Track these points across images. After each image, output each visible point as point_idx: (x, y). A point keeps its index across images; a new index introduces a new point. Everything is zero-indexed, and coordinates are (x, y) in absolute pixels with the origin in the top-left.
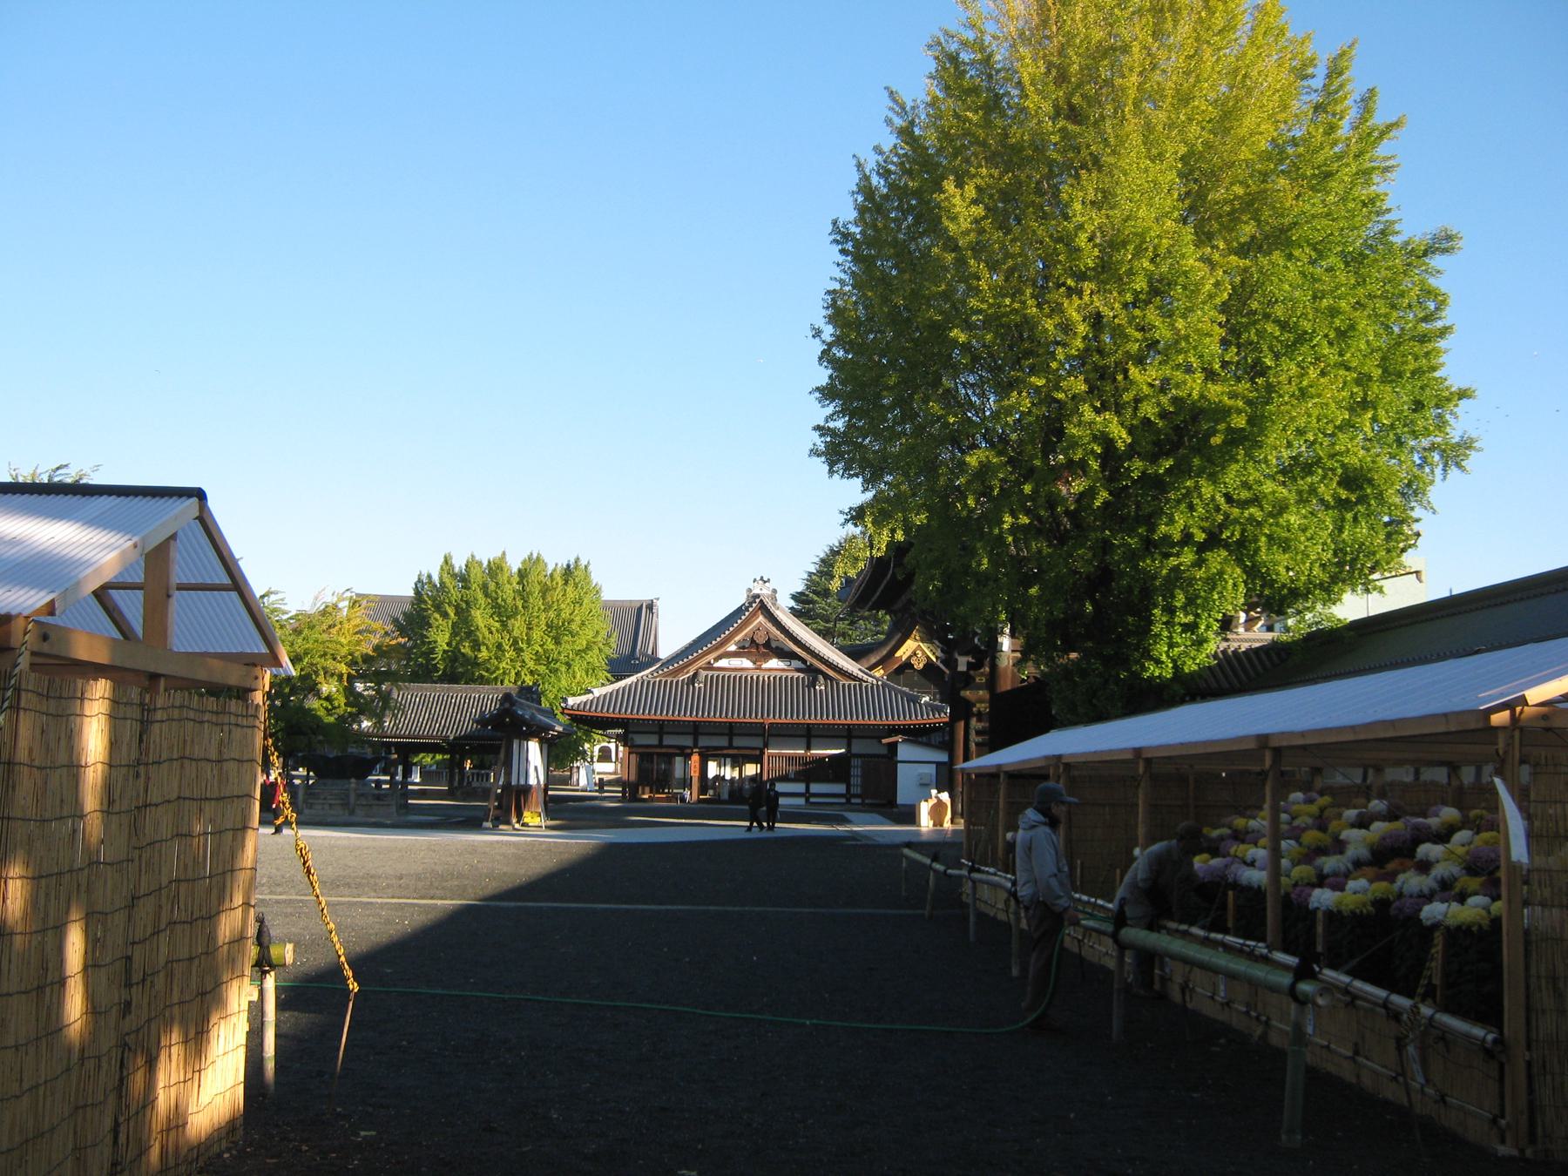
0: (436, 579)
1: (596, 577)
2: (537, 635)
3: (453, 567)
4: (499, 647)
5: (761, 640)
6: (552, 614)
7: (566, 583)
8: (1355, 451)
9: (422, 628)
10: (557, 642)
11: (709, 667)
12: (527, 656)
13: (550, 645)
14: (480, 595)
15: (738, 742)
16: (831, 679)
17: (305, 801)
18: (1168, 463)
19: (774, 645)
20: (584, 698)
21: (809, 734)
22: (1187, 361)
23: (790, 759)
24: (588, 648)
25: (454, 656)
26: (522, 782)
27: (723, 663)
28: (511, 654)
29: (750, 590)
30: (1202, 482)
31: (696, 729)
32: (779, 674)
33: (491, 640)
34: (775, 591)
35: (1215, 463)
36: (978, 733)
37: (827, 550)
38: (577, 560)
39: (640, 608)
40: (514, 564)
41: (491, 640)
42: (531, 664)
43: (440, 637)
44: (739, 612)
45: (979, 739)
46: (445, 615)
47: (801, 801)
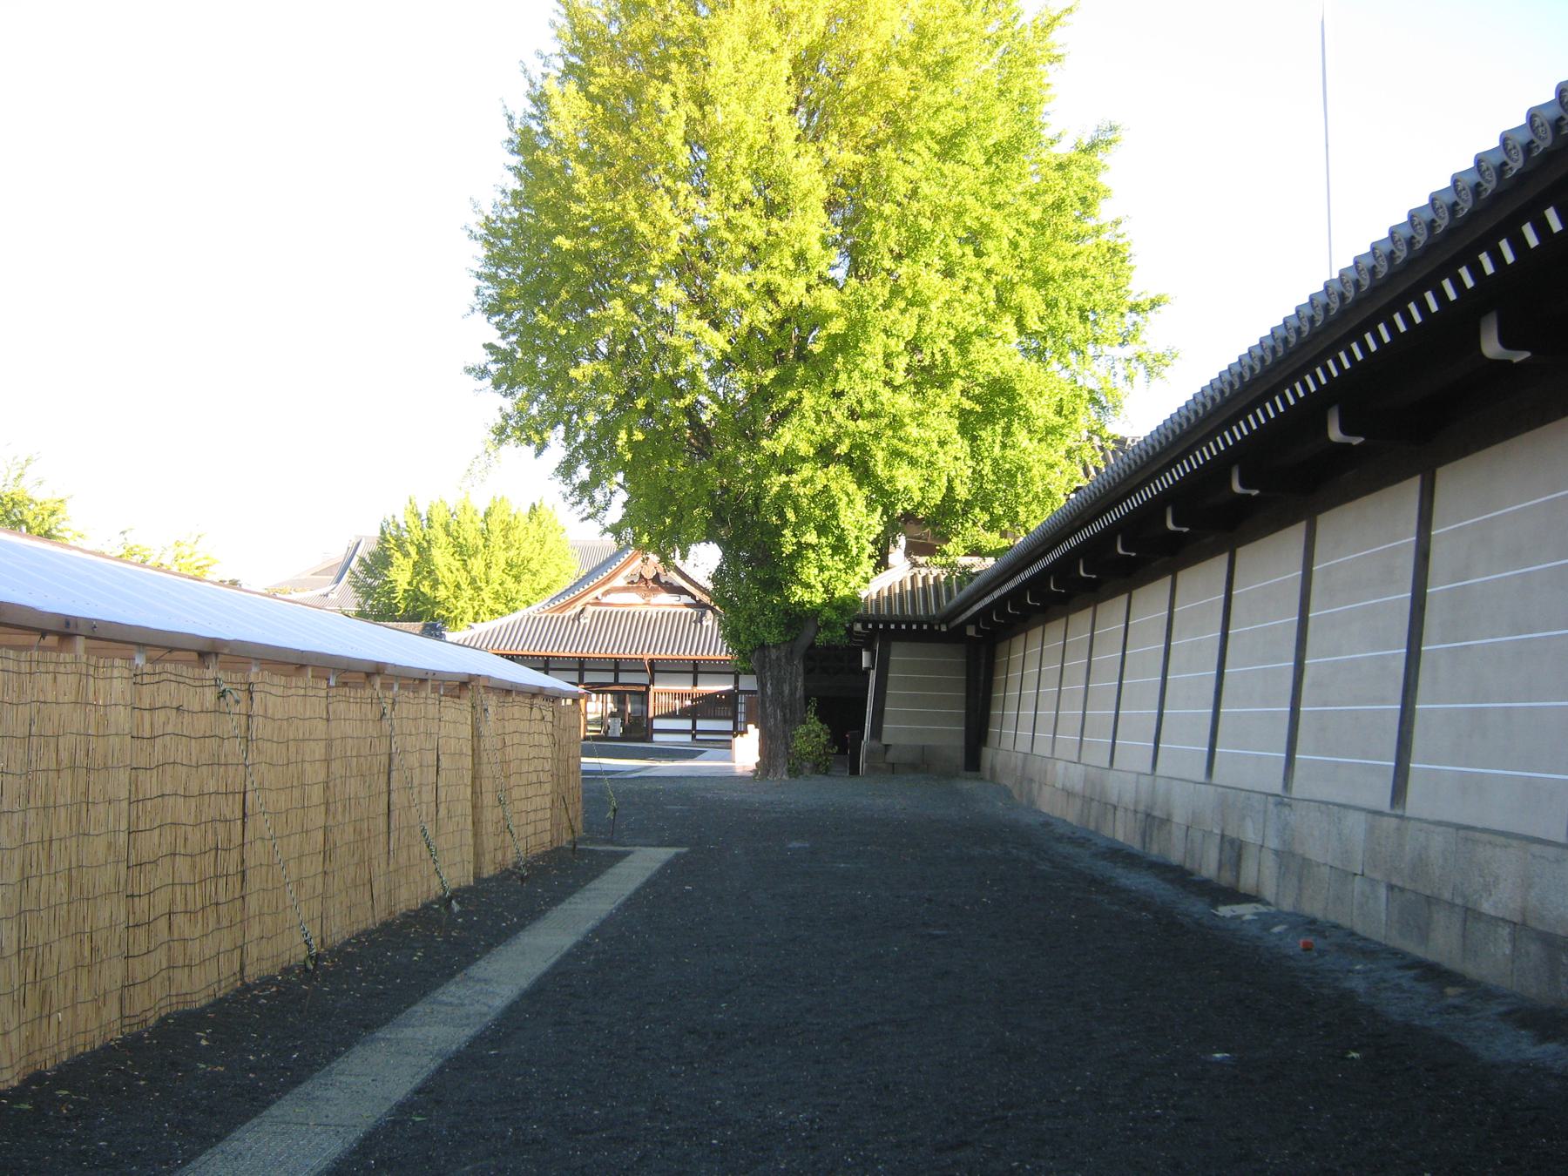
2: (495, 574)
4: (458, 586)
6: (513, 552)
8: (1000, 355)
9: (386, 568)
10: (517, 579)
13: (510, 583)
15: (623, 678)
18: (772, 374)
21: (696, 670)
22: (804, 265)
23: (682, 696)
25: (415, 596)
28: (468, 592)
30: (805, 393)
32: (667, 609)
35: (820, 369)
41: (449, 579)
42: (489, 603)
43: (401, 575)
46: (407, 555)
47: (688, 738)
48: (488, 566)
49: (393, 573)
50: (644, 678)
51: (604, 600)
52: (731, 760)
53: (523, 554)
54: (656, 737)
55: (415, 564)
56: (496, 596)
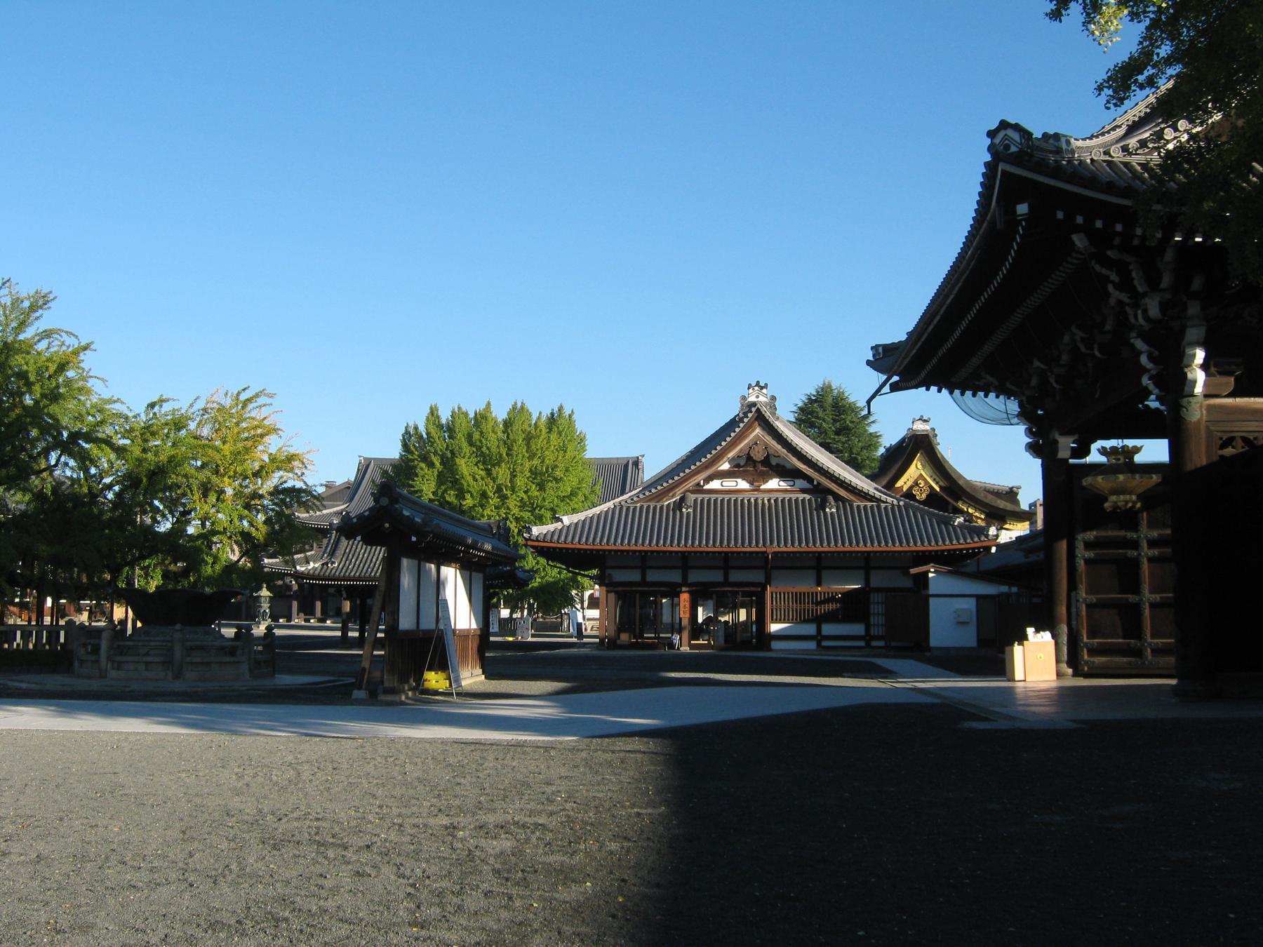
0: (422, 430)
1: (580, 426)
2: (520, 482)
3: (438, 417)
4: (484, 495)
5: (759, 455)
6: (535, 462)
7: (551, 430)
11: (698, 489)
12: (512, 503)
13: (535, 492)
14: (465, 444)
15: (735, 576)
17: (109, 658)
19: (774, 462)
20: (551, 527)
24: (573, 494)
26: (428, 623)
27: (715, 484)
28: (495, 501)
29: (744, 398)
31: (685, 561)
32: (781, 496)
33: (475, 487)
34: (773, 398)
36: (1088, 545)
38: (561, 408)
39: (626, 466)
40: (500, 413)
41: (475, 487)
42: (515, 511)
45: (1090, 554)
46: (431, 465)
47: (811, 645)
48: (513, 476)
49: (417, 483)
50: (758, 576)
52: (1012, 679)
54: (776, 645)
56: (523, 506)
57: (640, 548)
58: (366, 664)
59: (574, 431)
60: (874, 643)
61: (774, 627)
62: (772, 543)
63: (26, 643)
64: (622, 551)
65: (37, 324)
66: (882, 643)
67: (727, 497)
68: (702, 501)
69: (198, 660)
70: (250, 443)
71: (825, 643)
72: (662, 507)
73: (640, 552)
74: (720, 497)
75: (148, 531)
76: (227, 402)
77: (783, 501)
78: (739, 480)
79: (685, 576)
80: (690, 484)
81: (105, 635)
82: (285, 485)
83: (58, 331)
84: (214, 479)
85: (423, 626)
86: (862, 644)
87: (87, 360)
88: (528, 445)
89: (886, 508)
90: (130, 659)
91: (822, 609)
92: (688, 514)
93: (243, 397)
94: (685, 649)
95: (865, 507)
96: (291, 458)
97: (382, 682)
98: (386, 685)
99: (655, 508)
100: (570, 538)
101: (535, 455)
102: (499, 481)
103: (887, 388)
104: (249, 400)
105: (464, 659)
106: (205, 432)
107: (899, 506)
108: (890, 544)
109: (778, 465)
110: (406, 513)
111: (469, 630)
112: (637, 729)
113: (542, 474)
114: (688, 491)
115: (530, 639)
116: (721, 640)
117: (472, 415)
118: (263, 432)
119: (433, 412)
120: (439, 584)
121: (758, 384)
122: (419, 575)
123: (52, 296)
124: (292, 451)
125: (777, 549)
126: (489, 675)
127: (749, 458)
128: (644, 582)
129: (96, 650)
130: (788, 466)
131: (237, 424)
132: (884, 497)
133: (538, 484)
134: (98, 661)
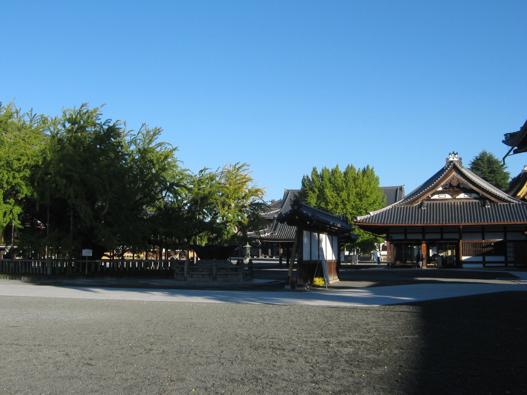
0: (310, 177)
1: (376, 174)
2: (352, 198)
3: (316, 172)
4: (336, 204)
5: (455, 184)
6: (358, 189)
7: (364, 176)
10: (361, 200)
11: (429, 199)
12: (348, 207)
13: (358, 202)
14: (328, 183)
15: (446, 236)
16: (493, 202)
17: (188, 273)
19: (462, 186)
20: (365, 217)
24: (374, 202)
26: (315, 258)
27: (436, 197)
28: (341, 206)
29: (447, 159)
31: (423, 230)
32: (465, 201)
33: (333, 201)
34: (461, 159)
37: (474, 158)
38: (368, 167)
39: (397, 190)
40: (342, 169)
41: (333, 201)
42: (350, 210)
44: (443, 170)
46: (314, 192)
47: (480, 266)
48: (349, 195)
49: (309, 200)
50: (456, 236)
51: (432, 198)
53: (363, 189)
54: (465, 266)
55: (318, 196)
56: (353, 208)
57: (404, 225)
58: (290, 275)
59: (374, 176)
60: (509, 265)
61: (464, 258)
62: (462, 221)
63: (156, 267)
64: (396, 226)
65: (156, 141)
66: (513, 265)
67: (441, 202)
68: (430, 204)
69: (222, 273)
70: (240, 185)
71: (487, 265)
72: (413, 207)
73: (404, 226)
74: (438, 202)
75: (202, 222)
76: (231, 169)
77: (466, 203)
78: (446, 195)
79: (424, 237)
80: (425, 197)
81: (186, 264)
82: (255, 202)
83: (164, 143)
84: (227, 200)
85: (313, 259)
86: (503, 265)
87: (176, 154)
88: (354, 182)
89: (513, 205)
90: (196, 273)
91: (485, 250)
92: (424, 210)
93: (237, 166)
94: (425, 268)
95: (503, 205)
96: (257, 191)
97: (297, 282)
98: (298, 283)
99: (410, 207)
100: (373, 221)
101: (357, 186)
102: (343, 198)
103: (512, 152)
104: (240, 168)
105: (330, 272)
106: (223, 181)
107: (519, 204)
108: (515, 221)
109: (464, 188)
110: (305, 212)
111: (332, 260)
112: (405, 302)
113: (361, 194)
114: (424, 200)
115: (357, 264)
116: (440, 264)
117: (330, 171)
118: (245, 180)
119: (314, 170)
120: (319, 241)
121: (453, 153)
122: (311, 238)
123: (161, 129)
124: (257, 188)
125: (464, 224)
126: (341, 279)
127: (451, 185)
128: (406, 239)
129: (183, 269)
130: (468, 188)
131: (235, 178)
132: (512, 200)
133: (359, 199)
134: (183, 274)
